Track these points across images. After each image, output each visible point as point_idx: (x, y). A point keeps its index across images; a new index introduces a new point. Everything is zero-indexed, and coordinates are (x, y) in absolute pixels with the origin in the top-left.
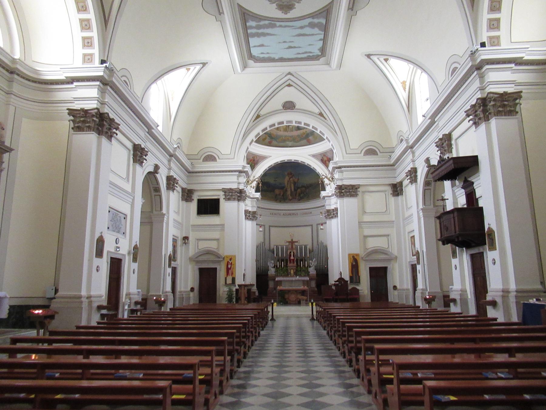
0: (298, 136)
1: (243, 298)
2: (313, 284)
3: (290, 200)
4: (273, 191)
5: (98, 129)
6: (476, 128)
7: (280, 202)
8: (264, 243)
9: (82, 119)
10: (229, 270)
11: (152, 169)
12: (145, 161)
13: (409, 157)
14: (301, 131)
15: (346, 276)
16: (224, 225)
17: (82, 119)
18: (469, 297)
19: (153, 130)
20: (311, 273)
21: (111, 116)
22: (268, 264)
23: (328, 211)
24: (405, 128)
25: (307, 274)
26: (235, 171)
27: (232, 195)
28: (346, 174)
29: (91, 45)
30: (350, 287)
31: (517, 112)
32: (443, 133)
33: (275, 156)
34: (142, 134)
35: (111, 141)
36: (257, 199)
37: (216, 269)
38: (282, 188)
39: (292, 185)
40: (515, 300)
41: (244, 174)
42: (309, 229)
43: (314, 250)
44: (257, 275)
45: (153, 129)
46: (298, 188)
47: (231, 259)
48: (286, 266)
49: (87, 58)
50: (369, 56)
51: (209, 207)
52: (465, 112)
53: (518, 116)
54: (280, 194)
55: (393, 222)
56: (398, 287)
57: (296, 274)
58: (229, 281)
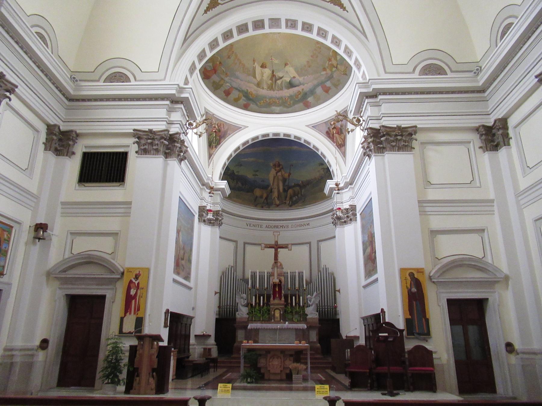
0: (291, 97)
1: (145, 370)
2: (314, 336)
3: (278, 206)
4: (250, 190)
7: (262, 208)
8: (234, 268)
10: (131, 301)
14: (296, 89)
15: (397, 317)
16: (130, 203)
20: (309, 316)
25: (303, 317)
27: (152, 144)
28: (385, 108)
30: (409, 345)
33: (253, 126)
36: (222, 190)
37: (103, 297)
38: (265, 187)
41: (182, 106)
42: (306, 248)
43: (313, 281)
44: (217, 320)
46: (290, 187)
47: (137, 277)
48: (268, 304)
51: (104, 168)
54: (261, 197)
55: (492, 201)
56: (517, 346)
57: (284, 318)
58: (129, 326)
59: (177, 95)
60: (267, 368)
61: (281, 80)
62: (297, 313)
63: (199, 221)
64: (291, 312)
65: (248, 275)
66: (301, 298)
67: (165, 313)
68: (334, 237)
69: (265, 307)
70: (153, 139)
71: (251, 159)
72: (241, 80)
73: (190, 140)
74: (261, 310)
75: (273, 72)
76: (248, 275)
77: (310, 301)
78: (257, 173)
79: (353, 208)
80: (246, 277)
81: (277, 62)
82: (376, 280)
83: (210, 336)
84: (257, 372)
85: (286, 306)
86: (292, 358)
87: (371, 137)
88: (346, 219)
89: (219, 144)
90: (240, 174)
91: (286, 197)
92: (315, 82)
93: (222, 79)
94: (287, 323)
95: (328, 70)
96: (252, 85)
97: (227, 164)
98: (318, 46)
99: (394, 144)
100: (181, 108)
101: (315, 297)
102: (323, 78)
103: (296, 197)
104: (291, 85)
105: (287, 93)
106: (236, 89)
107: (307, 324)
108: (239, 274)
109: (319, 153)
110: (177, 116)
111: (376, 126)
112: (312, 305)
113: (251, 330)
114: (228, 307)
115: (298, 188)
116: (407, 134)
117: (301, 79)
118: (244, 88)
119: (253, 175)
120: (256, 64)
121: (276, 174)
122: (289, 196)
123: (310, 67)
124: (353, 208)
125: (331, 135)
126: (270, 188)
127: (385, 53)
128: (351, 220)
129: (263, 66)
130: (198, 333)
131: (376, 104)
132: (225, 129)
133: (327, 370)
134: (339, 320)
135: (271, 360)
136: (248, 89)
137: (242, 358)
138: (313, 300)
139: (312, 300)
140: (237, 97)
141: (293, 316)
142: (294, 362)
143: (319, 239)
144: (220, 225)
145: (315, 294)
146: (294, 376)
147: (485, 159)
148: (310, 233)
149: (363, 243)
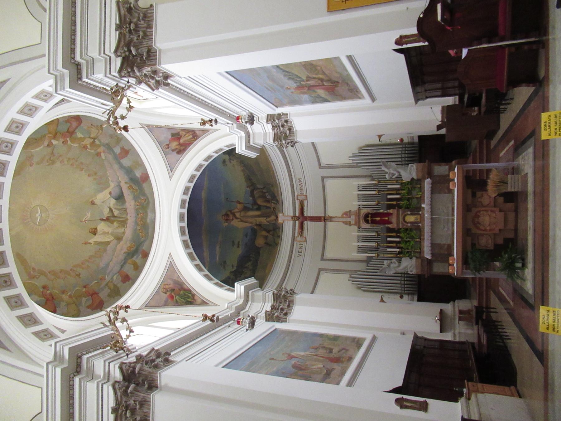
0: (136, 198)
2: (440, 169)
14: (126, 192)
22: (391, 273)
23: (277, 138)
25: (416, 183)
27: (133, 411)
33: (169, 246)
36: (247, 289)
38: (254, 232)
39: (251, 213)
41: (85, 357)
43: (369, 173)
46: (255, 203)
54: (266, 237)
57: (417, 210)
59: (66, 365)
60: (495, 235)
61: (114, 210)
62: (409, 192)
63: (286, 321)
64: (408, 200)
65: (364, 256)
66: (389, 186)
67: (402, 407)
68: (313, 143)
69: (402, 235)
70: (127, 407)
71: (218, 248)
72: (111, 260)
73: (173, 331)
74: (406, 240)
75: (102, 220)
76: (364, 256)
77: (393, 175)
78: (236, 242)
79: (271, 118)
80: (365, 259)
81: (89, 215)
82: (350, 58)
83: (441, 310)
84: (502, 249)
85: (400, 207)
86: (479, 194)
87: (133, 71)
88: (286, 129)
89: (190, 290)
90: (235, 264)
91: (268, 208)
92: (116, 167)
93: (107, 285)
94: (423, 206)
95: (99, 150)
96: (119, 247)
97: (216, 281)
98: (66, 162)
99: (141, 33)
100: (87, 358)
101: (389, 169)
102: (110, 157)
103: (267, 194)
104: (120, 198)
105: (130, 203)
106: (122, 267)
107: (424, 178)
108: (362, 267)
109: (206, 164)
110: (99, 367)
111: (119, 61)
112: (399, 172)
113: (433, 254)
114: (403, 282)
115: (255, 192)
116: (128, 16)
117: (112, 185)
118: (122, 257)
119: (238, 247)
120: (90, 241)
121: (237, 218)
122: (265, 204)
123: (96, 174)
124: (271, 118)
125: (182, 148)
126: (255, 227)
127: (26, 54)
128: (286, 121)
129: (94, 232)
130: (436, 327)
131: (90, 66)
132: (172, 283)
133: (492, 146)
134: (420, 137)
135: (482, 227)
136: (123, 252)
137: (478, 276)
138: (391, 170)
139: (392, 172)
140: (132, 266)
141: (413, 198)
142: (486, 191)
143: (318, 167)
144: (293, 292)
145: (383, 168)
146: (510, 188)
148: (310, 176)
149: (314, 102)
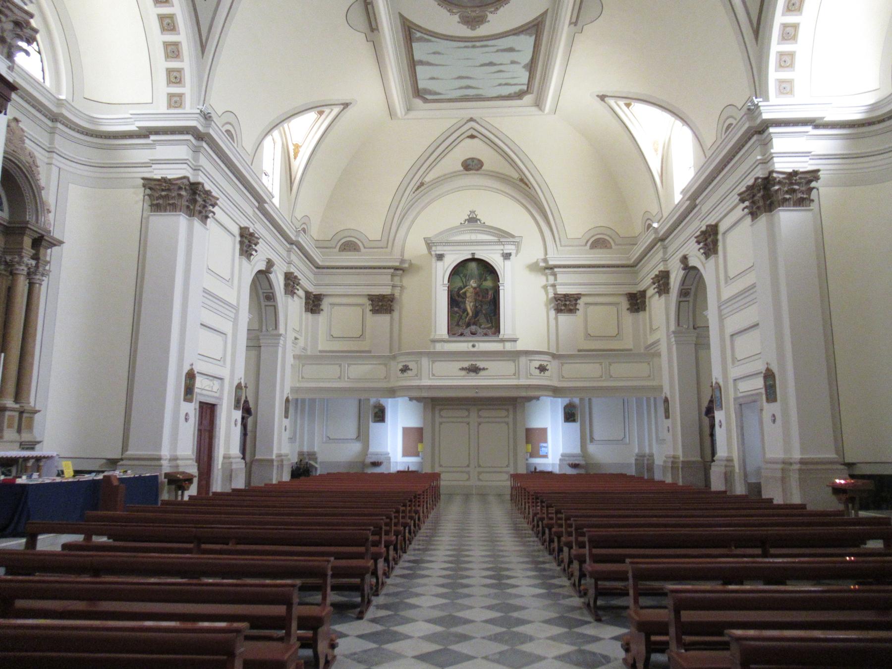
5: (188, 207)
6: (753, 220)
9: (163, 193)
11: (262, 266)
12: (254, 253)
13: (657, 256)
17: (163, 193)
18: (737, 470)
19: (266, 205)
21: (207, 187)
24: (654, 210)
26: (389, 268)
29: (180, 82)
31: (813, 201)
32: (708, 223)
34: (249, 211)
35: (205, 224)
40: (797, 476)
45: (266, 202)
49: (175, 101)
50: (602, 98)
52: (739, 195)
53: (813, 206)
147: (628, 318)
